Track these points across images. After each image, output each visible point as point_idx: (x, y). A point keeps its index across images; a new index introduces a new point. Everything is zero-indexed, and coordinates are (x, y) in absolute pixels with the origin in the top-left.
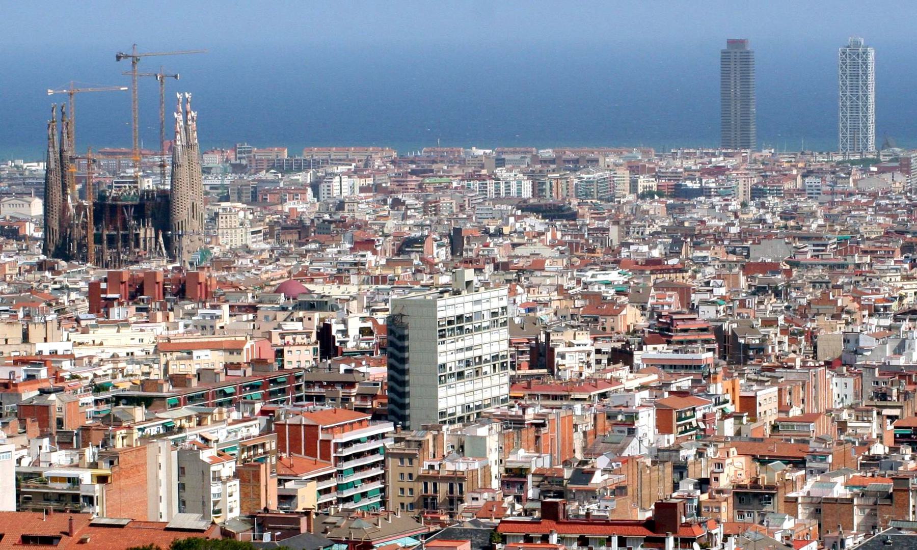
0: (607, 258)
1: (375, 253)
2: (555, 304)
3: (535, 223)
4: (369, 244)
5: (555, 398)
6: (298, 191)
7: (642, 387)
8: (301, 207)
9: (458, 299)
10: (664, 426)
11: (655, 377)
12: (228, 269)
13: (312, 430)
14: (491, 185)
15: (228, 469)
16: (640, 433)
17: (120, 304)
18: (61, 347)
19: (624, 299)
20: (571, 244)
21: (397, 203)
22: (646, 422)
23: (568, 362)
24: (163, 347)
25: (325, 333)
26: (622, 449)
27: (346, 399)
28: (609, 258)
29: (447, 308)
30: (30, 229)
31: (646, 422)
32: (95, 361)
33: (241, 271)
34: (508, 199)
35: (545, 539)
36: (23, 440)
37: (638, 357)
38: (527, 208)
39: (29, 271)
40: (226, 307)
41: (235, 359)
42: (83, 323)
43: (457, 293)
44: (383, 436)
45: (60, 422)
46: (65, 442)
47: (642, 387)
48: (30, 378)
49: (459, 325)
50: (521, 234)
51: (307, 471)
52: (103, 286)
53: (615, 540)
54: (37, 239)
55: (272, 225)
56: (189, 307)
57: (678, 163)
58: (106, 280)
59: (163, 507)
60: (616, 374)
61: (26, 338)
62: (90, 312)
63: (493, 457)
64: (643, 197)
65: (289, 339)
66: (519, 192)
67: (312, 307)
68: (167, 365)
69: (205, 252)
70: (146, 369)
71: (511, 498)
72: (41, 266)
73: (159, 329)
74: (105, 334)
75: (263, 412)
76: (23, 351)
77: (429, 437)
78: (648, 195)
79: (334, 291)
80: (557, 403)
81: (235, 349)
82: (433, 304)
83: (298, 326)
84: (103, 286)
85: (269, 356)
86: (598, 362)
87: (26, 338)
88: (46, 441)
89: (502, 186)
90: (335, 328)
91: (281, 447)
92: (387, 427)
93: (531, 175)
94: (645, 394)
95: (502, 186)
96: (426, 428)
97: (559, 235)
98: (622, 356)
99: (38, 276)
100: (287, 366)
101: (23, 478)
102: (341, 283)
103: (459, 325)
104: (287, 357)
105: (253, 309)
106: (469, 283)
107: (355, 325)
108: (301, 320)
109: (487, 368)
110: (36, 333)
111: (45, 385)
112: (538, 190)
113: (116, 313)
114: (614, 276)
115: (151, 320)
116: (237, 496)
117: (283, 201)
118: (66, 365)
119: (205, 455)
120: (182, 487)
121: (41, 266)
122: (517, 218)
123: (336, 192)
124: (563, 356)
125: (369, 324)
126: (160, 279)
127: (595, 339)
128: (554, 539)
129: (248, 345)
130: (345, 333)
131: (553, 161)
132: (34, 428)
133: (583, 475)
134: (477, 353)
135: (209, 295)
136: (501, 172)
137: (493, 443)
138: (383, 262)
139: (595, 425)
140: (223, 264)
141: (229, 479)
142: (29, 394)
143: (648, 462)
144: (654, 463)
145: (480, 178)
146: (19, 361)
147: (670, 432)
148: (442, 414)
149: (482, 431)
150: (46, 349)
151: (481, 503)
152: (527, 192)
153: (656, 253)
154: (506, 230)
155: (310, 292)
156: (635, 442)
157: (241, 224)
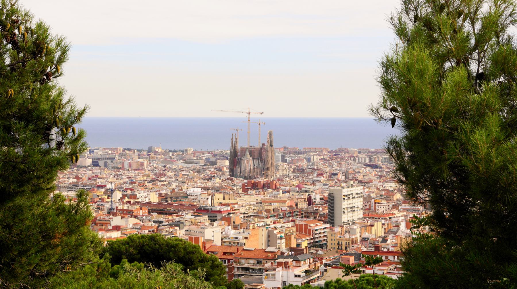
4: (322, 175)
5: (376, 218)
7: (401, 216)
8: (302, 164)
11: (405, 213)
37: (400, 207)
38: (367, 165)
39: (225, 180)
40: (281, 191)
45: (234, 222)
46: (235, 228)
47: (401, 216)
52: (246, 184)
55: (294, 169)
67: (306, 191)
74: (247, 197)
80: (377, 220)
82: (342, 191)
86: (389, 209)
91: (297, 231)
93: (368, 156)
94: (403, 218)
98: (395, 207)
102: (314, 185)
104: (299, 206)
107: (318, 197)
110: (227, 197)
112: (370, 160)
122: (365, 168)
125: (322, 197)
126: (262, 183)
131: (374, 152)
137: (358, 230)
139: (388, 226)
149: (355, 227)
152: (367, 161)
154: (361, 172)
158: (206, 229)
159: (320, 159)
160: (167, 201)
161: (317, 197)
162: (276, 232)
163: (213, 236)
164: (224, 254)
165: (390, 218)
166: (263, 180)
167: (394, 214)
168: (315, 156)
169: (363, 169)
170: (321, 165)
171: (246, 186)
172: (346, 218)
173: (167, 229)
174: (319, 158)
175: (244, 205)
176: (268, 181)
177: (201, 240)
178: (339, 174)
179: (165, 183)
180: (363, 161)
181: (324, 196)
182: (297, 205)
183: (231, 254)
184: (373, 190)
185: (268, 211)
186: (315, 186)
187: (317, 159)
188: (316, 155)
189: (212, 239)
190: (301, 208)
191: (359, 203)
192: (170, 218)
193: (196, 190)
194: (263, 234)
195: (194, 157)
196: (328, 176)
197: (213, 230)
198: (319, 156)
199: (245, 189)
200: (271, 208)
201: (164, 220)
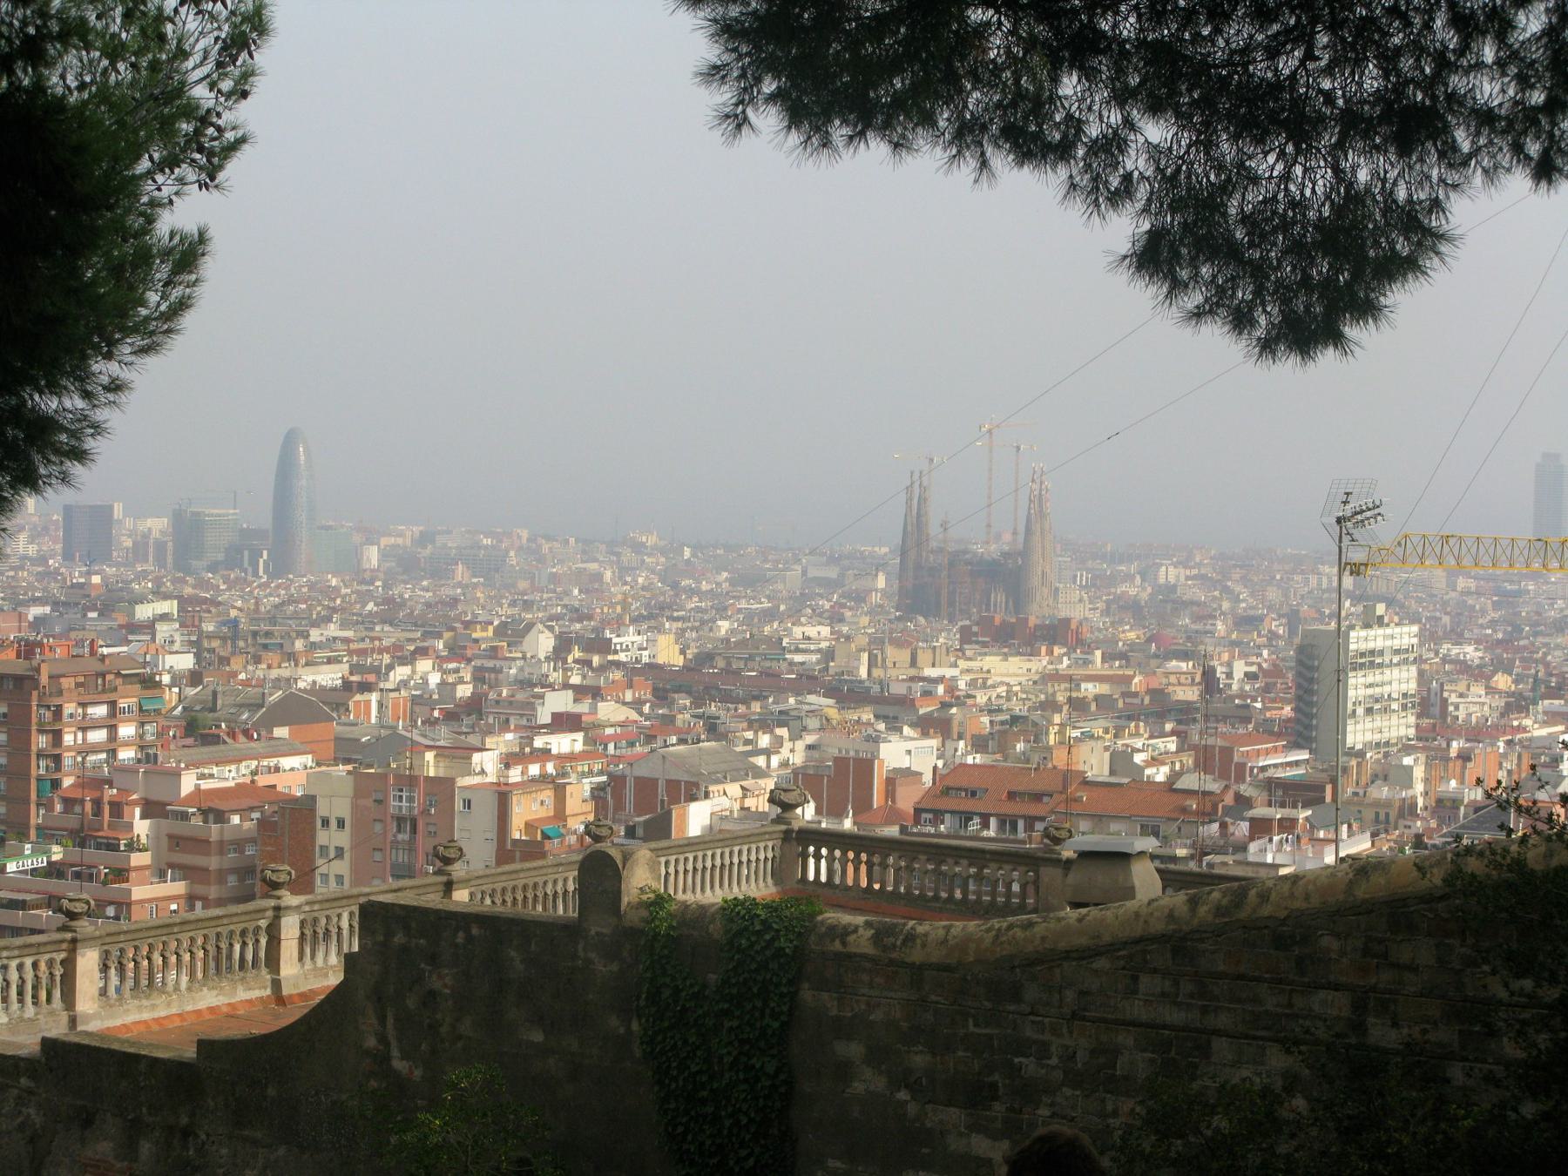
14: (1313, 580)
21: (1226, 590)
25: (1209, 676)
40: (1098, 653)
44: (1297, 763)
65: (1173, 679)
90: (1220, 671)
109: (1395, 706)
110: (924, 657)
124: (1457, 708)
125: (1254, 669)
129: (1136, 680)
130: (1229, 675)
137: (1419, 773)
139: (1519, 765)
145: (1302, 572)
167: (1524, 729)
172: (1357, 734)
174: (1183, 572)
178: (1267, 620)
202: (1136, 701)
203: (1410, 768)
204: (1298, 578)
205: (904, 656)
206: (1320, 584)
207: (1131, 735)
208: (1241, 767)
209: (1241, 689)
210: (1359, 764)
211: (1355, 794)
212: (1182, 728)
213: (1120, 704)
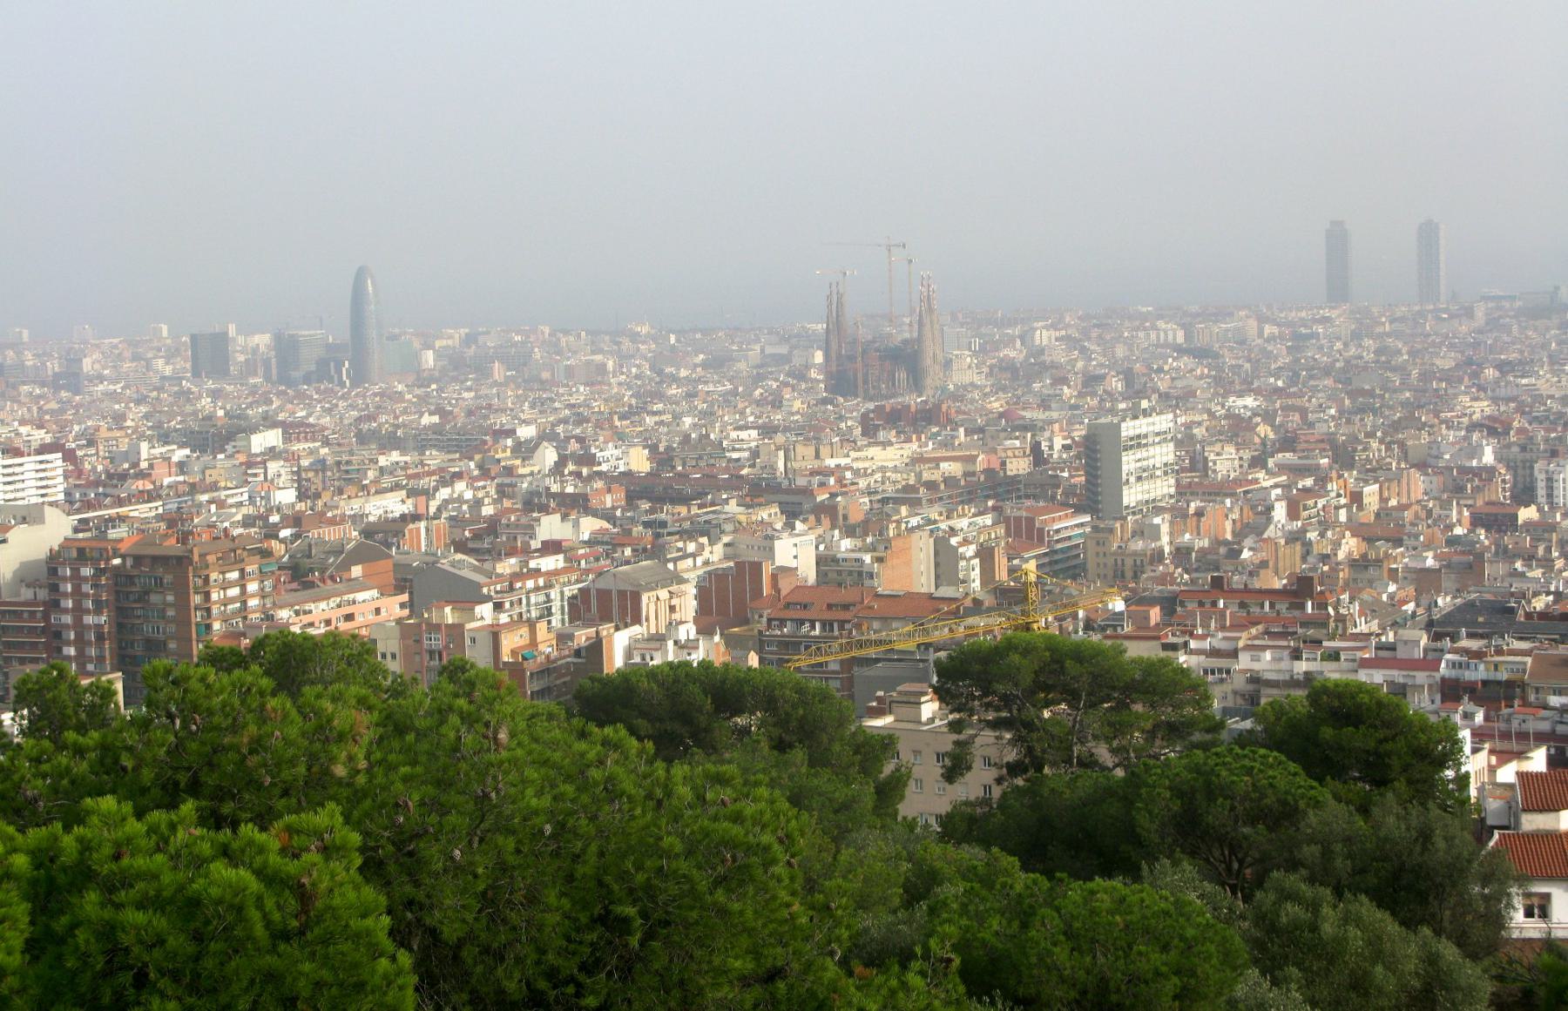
0: (1244, 387)
1: (1069, 387)
2: (1206, 424)
3: (1185, 362)
4: (1064, 381)
5: (1210, 494)
6: (1010, 341)
7: (1276, 486)
8: (1013, 354)
9: (1137, 422)
10: (1293, 514)
11: (1285, 478)
12: (962, 401)
13: (1030, 521)
14: (1153, 336)
15: (970, 550)
16: (1276, 519)
17: (884, 429)
18: (843, 461)
19: (1259, 419)
20: (1215, 377)
21: (1083, 350)
22: (1280, 512)
23: (1218, 467)
24: (917, 460)
25: (1036, 449)
26: (1263, 533)
27: (1053, 497)
28: (1244, 387)
29: (1129, 428)
30: (813, 374)
31: (1280, 512)
32: (869, 471)
33: (973, 401)
34: (1166, 345)
35: (1214, 604)
36: (820, 531)
37: (1271, 463)
38: (1181, 351)
39: (816, 405)
40: (962, 430)
41: (970, 468)
42: (859, 443)
43: (1135, 417)
44: (1082, 525)
45: (845, 517)
46: (850, 532)
47: (1276, 486)
48: (822, 485)
49: (1138, 442)
50: (1178, 369)
51: (1028, 550)
52: (872, 415)
53: (1267, 604)
54: (819, 381)
55: (991, 367)
56: (935, 430)
57: (1293, 314)
58: (873, 411)
59: (923, 580)
60: (1257, 475)
61: (817, 456)
62: (863, 435)
63: (1165, 539)
64: (1268, 340)
65: (1010, 453)
66: (1175, 338)
67: (1025, 428)
68: (921, 472)
69: (944, 389)
70: (905, 476)
71: (1180, 570)
72: (824, 401)
73: (914, 446)
74: (873, 451)
75: (994, 508)
76: (816, 464)
77: (1118, 525)
78: (1271, 339)
79: (1040, 415)
80: (1213, 498)
81: (973, 459)
82: (1118, 426)
83: (1017, 443)
84: (872, 415)
85: (996, 465)
86: (1241, 466)
87: (817, 456)
88: (837, 532)
89: (1162, 334)
90: (1044, 446)
91: (1008, 534)
92: (1087, 518)
93: (1183, 326)
94: (1279, 491)
95: (1162, 334)
96: (1116, 519)
97: (1206, 371)
98: (1258, 462)
99: (823, 408)
100: (1009, 473)
101: (820, 561)
102: (1045, 410)
103: (1138, 442)
104: (1009, 466)
105: (981, 430)
106: (1145, 410)
107: (1058, 442)
108: (1017, 438)
109: (1158, 473)
110: (824, 451)
111: (833, 490)
112: (1188, 337)
113: (882, 435)
114: (1250, 401)
115: (908, 440)
116: (978, 570)
117: (998, 350)
118: (848, 475)
119: (954, 541)
120: (937, 565)
121: (824, 401)
122: (1175, 359)
123: (1037, 342)
124: (1215, 463)
125: (1069, 442)
126: (913, 409)
127: (1238, 450)
128: (1221, 604)
129: (980, 458)
130: (1051, 448)
131: (1198, 315)
132: (826, 521)
133: (1235, 553)
134: (1151, 462)
135: (950, 421)
136: (1161, 324)
137: (1165, 529)
138: (1075, 393)
139: (1241, 514)
140: (956, 397)
141: (971, 558)
142: (822, 497)
143: (1282, 542)
144: (1287, 543)
145: (1145, 329)
146: (813, 473)
147: (1298, 519)
148: (1127, 507)
149: (1157, 520)
150: (831, 463)
151: (1158, 574)
152: (1180, 338)
153: (1280, 383)
154: (1166, 368)
155: (1023, 418)
156: (1272, 527)
157: (969, 367)
158: (779, 538)
159: (1057, 339)
160: (674, 467)
161: (1056, 444)
162: (954, 541)
163: (795, 557)
164: (830, 606)
165: (1246, 492)
166: (914, 401)
167: (1256, 481)
168: (1044, 332)
169: (1170, 360)
170: (1060, 355)
171: (872, 419)
172: (1132, 496)
173: (680, 544)
174: (1054, 334)
175: (869, 471)
176: (925, 402)
177: (767, 570)
178: (1108, 377)
179: (664, 418)
180: (1170, 337)
181: (1073, 439)
182: (1003, 464)
183: (846, 607)
184: (1197, 418)
185: (931, 486)
186: (1047, 413)
187: (1050, 338)
188: (1047, 328)
189: (793, 564)
190: (1015, 472)
191: (1164, 454)
192: (683, 510)
193: (744, 435)
194: (922, 549)
195: (733, 343)
196: (1079, 381)
197: (796, 540)
198: (1056, 330)
199: (869, 430)
200: (936, 476)
201: (669, 518)
202: (975, 479)
203: (1158, 526)
204: (1142, 334)
205: (811, 451)
206: (1158, 337)
207: (959, 516)
208: (1041, 531)
209: (1060, 457)
210: (1122, 526)
211: (1120, 547)
212: (1000, 504)
213: (963, 483)
